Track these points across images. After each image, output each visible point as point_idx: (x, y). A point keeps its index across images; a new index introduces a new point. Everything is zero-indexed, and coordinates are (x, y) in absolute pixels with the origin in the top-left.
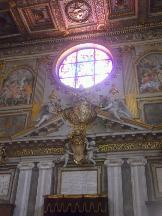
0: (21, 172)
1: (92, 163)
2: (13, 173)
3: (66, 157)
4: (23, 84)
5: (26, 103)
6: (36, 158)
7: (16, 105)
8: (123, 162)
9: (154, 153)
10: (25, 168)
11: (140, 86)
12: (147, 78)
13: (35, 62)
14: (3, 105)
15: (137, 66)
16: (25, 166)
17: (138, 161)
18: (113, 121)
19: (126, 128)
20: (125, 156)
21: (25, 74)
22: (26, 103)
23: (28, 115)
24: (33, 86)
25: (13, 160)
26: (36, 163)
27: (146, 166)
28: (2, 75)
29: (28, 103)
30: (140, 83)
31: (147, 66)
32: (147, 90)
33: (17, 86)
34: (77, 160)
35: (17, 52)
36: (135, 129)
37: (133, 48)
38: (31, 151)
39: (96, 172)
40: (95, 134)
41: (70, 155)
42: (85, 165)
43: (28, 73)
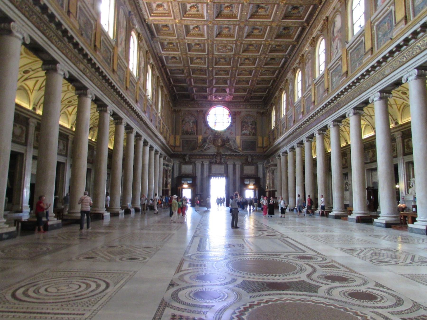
0: (197, 165)
1: (223, 163)
5: (194, 134)
9: (244, 161)
12: (244, 128)
19: (236, 152)
24: (197, 126)
25: (193, 160)
26: (202, 162)
27: (241, 165)
30: (242, 130)
32: (244, 134)
34: (218, 161)
37: (240, 112)
42: (220, 163)
43: (193, 118)
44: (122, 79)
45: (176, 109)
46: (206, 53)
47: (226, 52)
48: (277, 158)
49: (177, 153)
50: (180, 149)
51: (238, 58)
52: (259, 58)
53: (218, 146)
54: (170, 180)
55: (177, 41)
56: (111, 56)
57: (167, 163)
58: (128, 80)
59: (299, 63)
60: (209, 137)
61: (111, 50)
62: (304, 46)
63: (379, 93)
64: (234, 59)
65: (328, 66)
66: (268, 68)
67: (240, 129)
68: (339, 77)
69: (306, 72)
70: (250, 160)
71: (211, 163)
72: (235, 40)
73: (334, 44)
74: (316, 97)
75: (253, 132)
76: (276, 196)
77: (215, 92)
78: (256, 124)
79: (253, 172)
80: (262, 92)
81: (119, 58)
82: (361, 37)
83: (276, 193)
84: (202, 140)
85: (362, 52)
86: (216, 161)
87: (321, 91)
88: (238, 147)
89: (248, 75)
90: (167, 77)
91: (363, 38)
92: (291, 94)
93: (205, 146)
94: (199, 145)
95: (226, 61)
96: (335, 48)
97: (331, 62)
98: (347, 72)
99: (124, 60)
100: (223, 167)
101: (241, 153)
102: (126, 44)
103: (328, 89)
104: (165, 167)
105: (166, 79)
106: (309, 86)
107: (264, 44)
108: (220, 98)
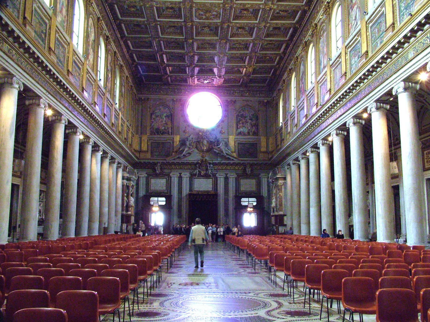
0: (173, 178)
1: (210, 175)
2: (167, 178)
3: (197, 171)
4: (165, 119)
6: (180, 171)
7: (162, 134)
8: (225, 176)
9: (240, 172)
10: (175, 176)
11: (237, 130)
12: (241, 125)
13: (171, 102)
14: (153, 134)
15: (237, 116)
16: (174, 175)
17: (232, 176)
18: (222, 154)
19: (229, 159)
20: (226, 173)
21: (165, 111)
22: (168, 134)
23: (171, 143)
25: (166, 171)
26: (180, 174)
27: (236, 178)
28: (149, 110)
29: (170, 134)
31: (242, 116)
32: (240, 134)
33: (161, 120)
34: (203, 173)
35: (157, 91)
36: (233, 160)
37: (235, 102)
38: (177, 166)
39: (211, 180)
40: (213, 161)
41: (199, 171)
42: (207, 176)
44: (62, 59)
45: (143, 97)
46: (183, 20)
47: (211, 19)
48: (286, 167)
49: (142, 161)
50: (149, 155)
51: (228, 26)
52: (258, 27)
53: (203, 151)
54: (132, 200)
55: (142, 4)
56: (46, 31)
57: (128, 175)
58: (71, 61)
59: (312, 36)
60: (190, 138)
61: (47, 21)
62: (318, 12)
63: (403, 83)
64: (222, 28)
65: (345, 42)
66: (271, 41)
67: (235, 125)
68: (359, 58)
69: (321, 48)
70: (248, 170)
71: (192, 176)
72: (222, 3)
73: (353, 14)
74: (332, 83)
75: (253, 130)
76: (285, 223)
77: (198, 73)
78: (257, 119)
79: (254, 189)
80: (266, 73)
81: (58, 31)
82: (382, 8)
83: (285, 218)
84: (180, 141)
85: (383, 28)
86: (200, 172)
87: (338, 76)
88: (232, 152)
89: (244, 50)
90: (128, 52)
91: (384, 9)
92: (302, 77)
93: (183, 150)
94: (175, 150)
95: (211, 30)
96: (354, 18)
97: (349, 37)
98: (367, 52)
99: (64, 33)
100: (210, 181)
101: (236, 161)
102: (67, 11)
103: (346, 73)
104: (125, 181)
105: (127, 56)
106: (324, 67)
107: (263, 9)
108: (206, 82)
